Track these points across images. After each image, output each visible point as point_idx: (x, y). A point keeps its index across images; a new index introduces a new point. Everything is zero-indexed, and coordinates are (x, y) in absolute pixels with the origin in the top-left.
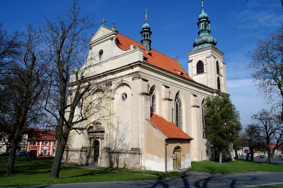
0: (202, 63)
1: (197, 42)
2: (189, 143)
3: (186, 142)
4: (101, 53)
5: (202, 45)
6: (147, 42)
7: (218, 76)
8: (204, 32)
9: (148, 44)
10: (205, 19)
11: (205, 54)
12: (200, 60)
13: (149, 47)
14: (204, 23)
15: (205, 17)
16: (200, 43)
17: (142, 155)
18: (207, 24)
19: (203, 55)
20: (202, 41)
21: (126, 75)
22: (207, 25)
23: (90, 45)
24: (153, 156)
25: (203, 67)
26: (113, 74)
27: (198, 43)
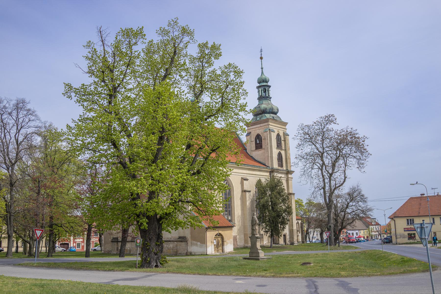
2: (232, 230)
3: (228, 229)
5: (260, 116)
7: (279, 151)
8: (264, 99)
11: (263, 127)
14: (263, 88)
17: (188, 242)
19: (261, 128)
20: (260, 111)
24: (196, 242)
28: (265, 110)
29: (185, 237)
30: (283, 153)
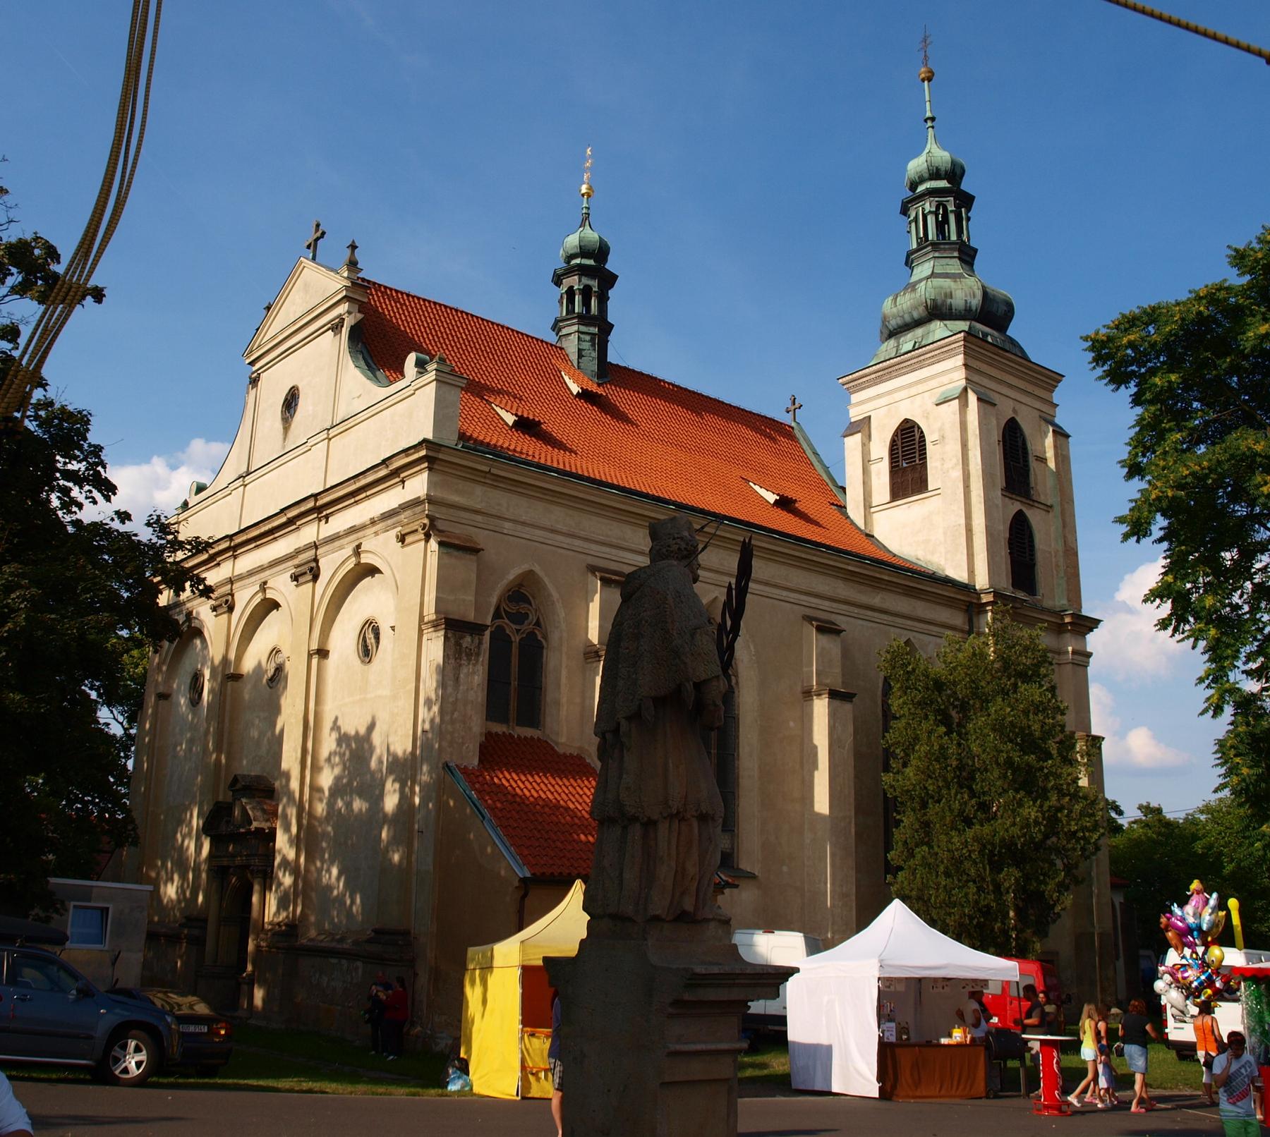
0: (917, 437)
1: (894, 317)
4: (291, 402)
5: (919, 332)
6: (583, 329)
7: (1015, 507)
8: (937, 255)
9: (588, 338)
10: (943, 184)
11: (933, 383)
12: (906, 421)
13: (595, 354)
14: (934, 204)
15: (938, 169)
16: (907, 318)
18: (951, 208)
19: (921, 388)
21: (373, 522)
22: (952, 218)
23: (252, 363)
25: (926, 458)
26: (327, 517)
27: (899, 321)
28: (944, 301)
29: (406, 933)
30: (1034, 516)
